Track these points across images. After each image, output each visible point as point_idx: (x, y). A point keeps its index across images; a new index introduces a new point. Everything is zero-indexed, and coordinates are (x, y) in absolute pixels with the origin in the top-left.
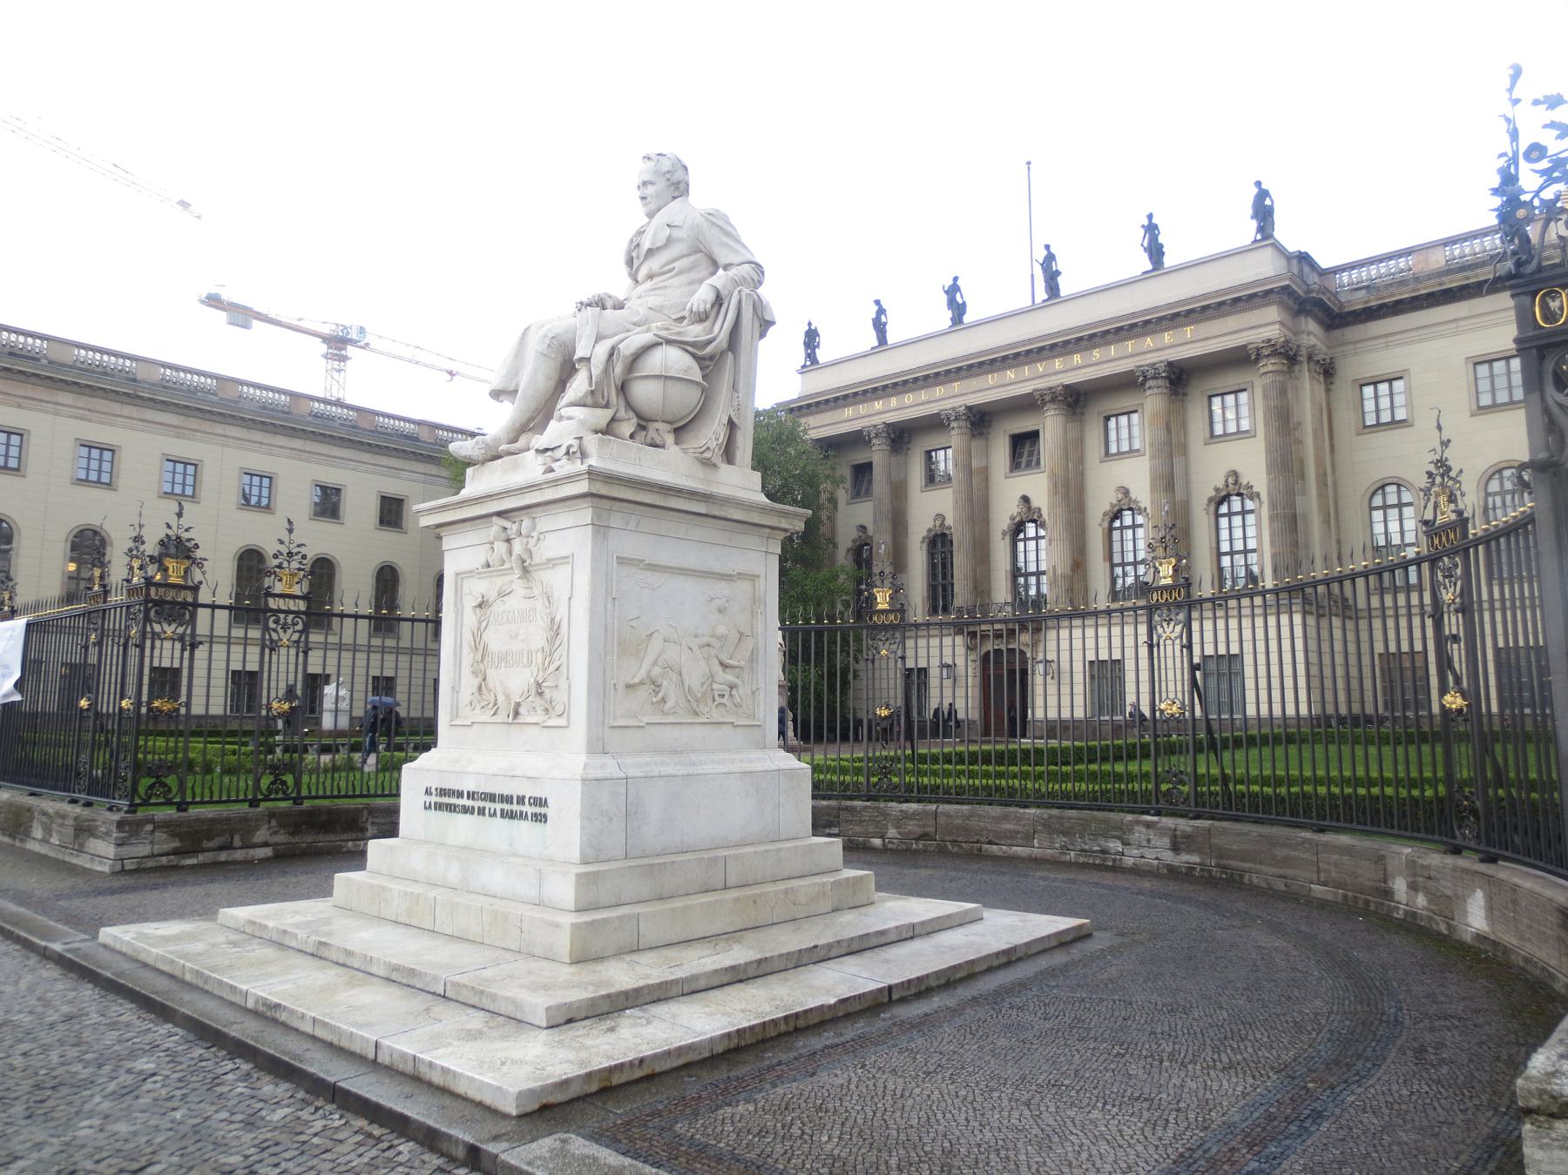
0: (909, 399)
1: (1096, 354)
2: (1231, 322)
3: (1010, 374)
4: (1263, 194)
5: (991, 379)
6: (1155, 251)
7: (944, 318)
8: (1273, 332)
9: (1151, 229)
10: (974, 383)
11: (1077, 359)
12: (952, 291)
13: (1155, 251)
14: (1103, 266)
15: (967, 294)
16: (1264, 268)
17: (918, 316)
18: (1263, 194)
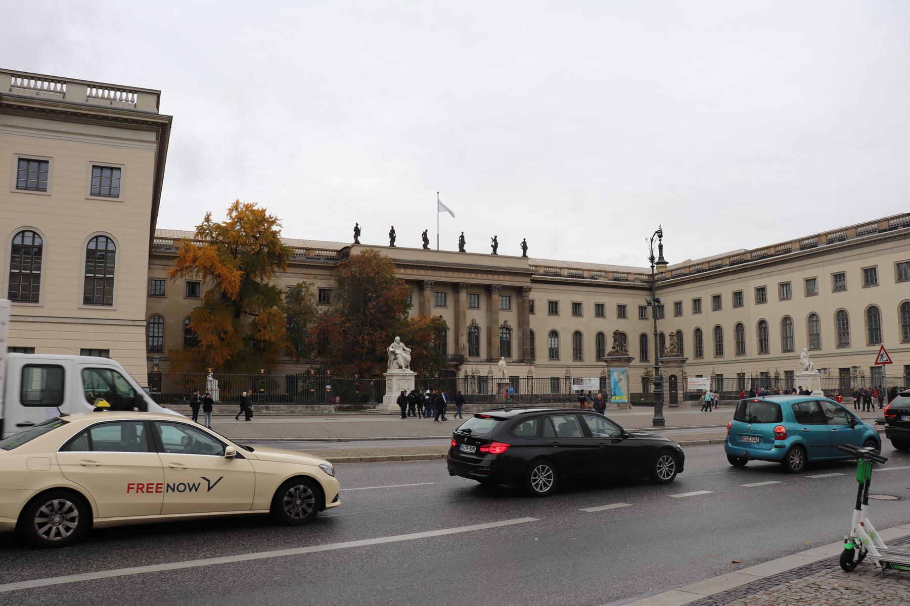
0: (409, 271)
1: (480, 276)
2: (519, 279)
3: (450, 274)
4: (524, 243)
5: (443, 273)
6: (495, 247)
7: (420, 245)
8: (529, 285)
9: (495, 240)
10: (436, 273)
11: (473, 275)
12: (425, 234)
13: (495, 247)
14: (478, 246)
15: (429, 237)
16: (523, 265)
17: (409, 240)
18: (524, 243)
